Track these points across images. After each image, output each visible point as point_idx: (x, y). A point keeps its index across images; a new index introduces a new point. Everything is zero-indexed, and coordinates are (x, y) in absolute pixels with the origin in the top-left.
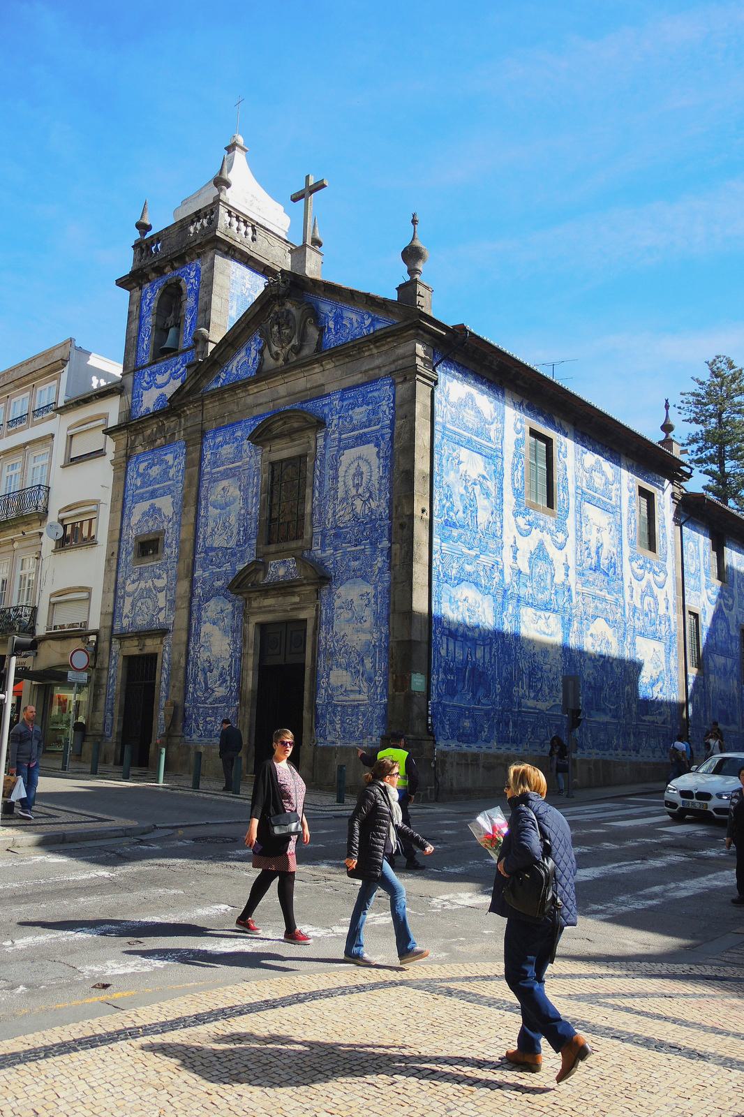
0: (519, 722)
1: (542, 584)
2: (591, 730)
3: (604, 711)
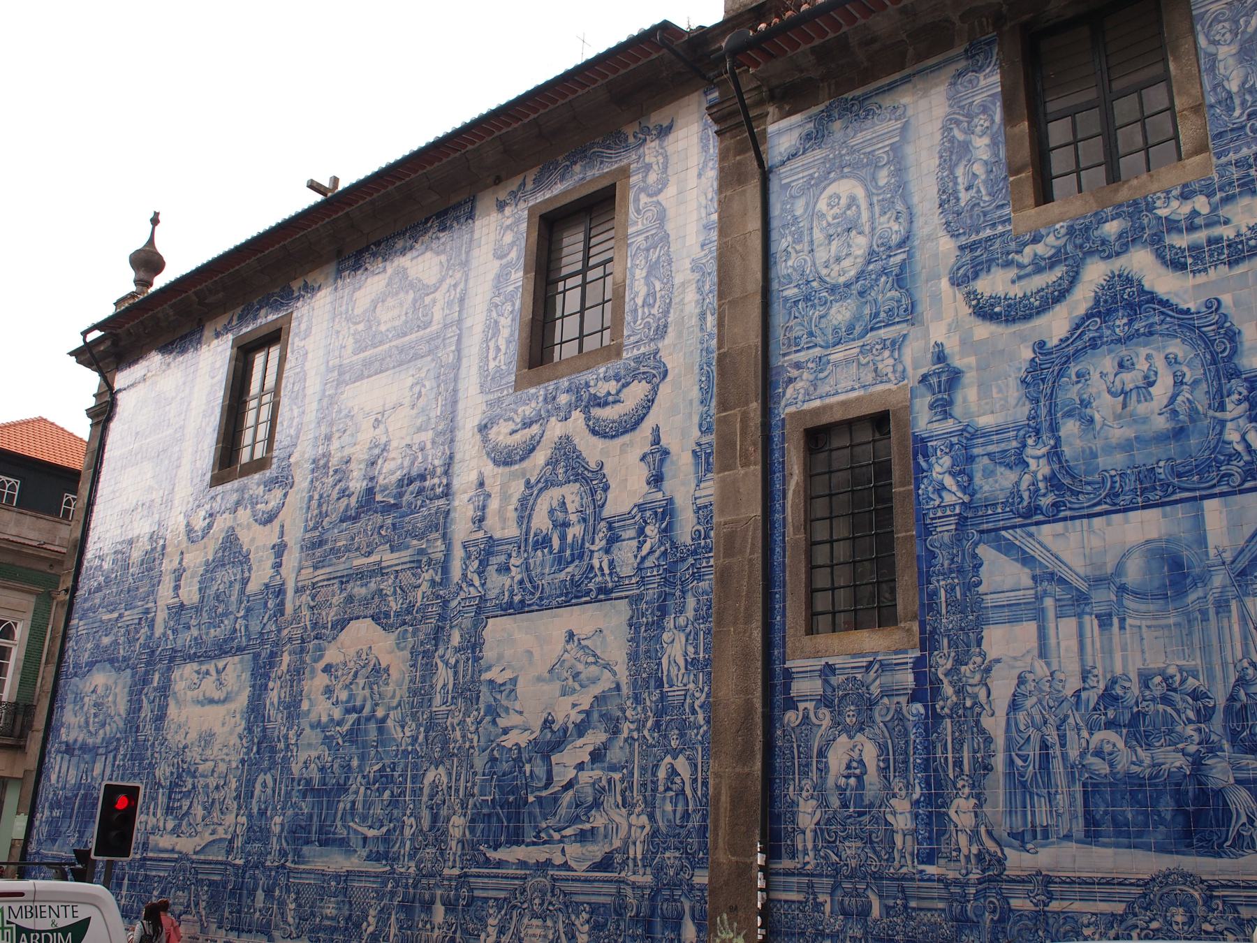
0: (140, 878)
1: (220, 610)
2: (298, 893)
3: (343, 843)
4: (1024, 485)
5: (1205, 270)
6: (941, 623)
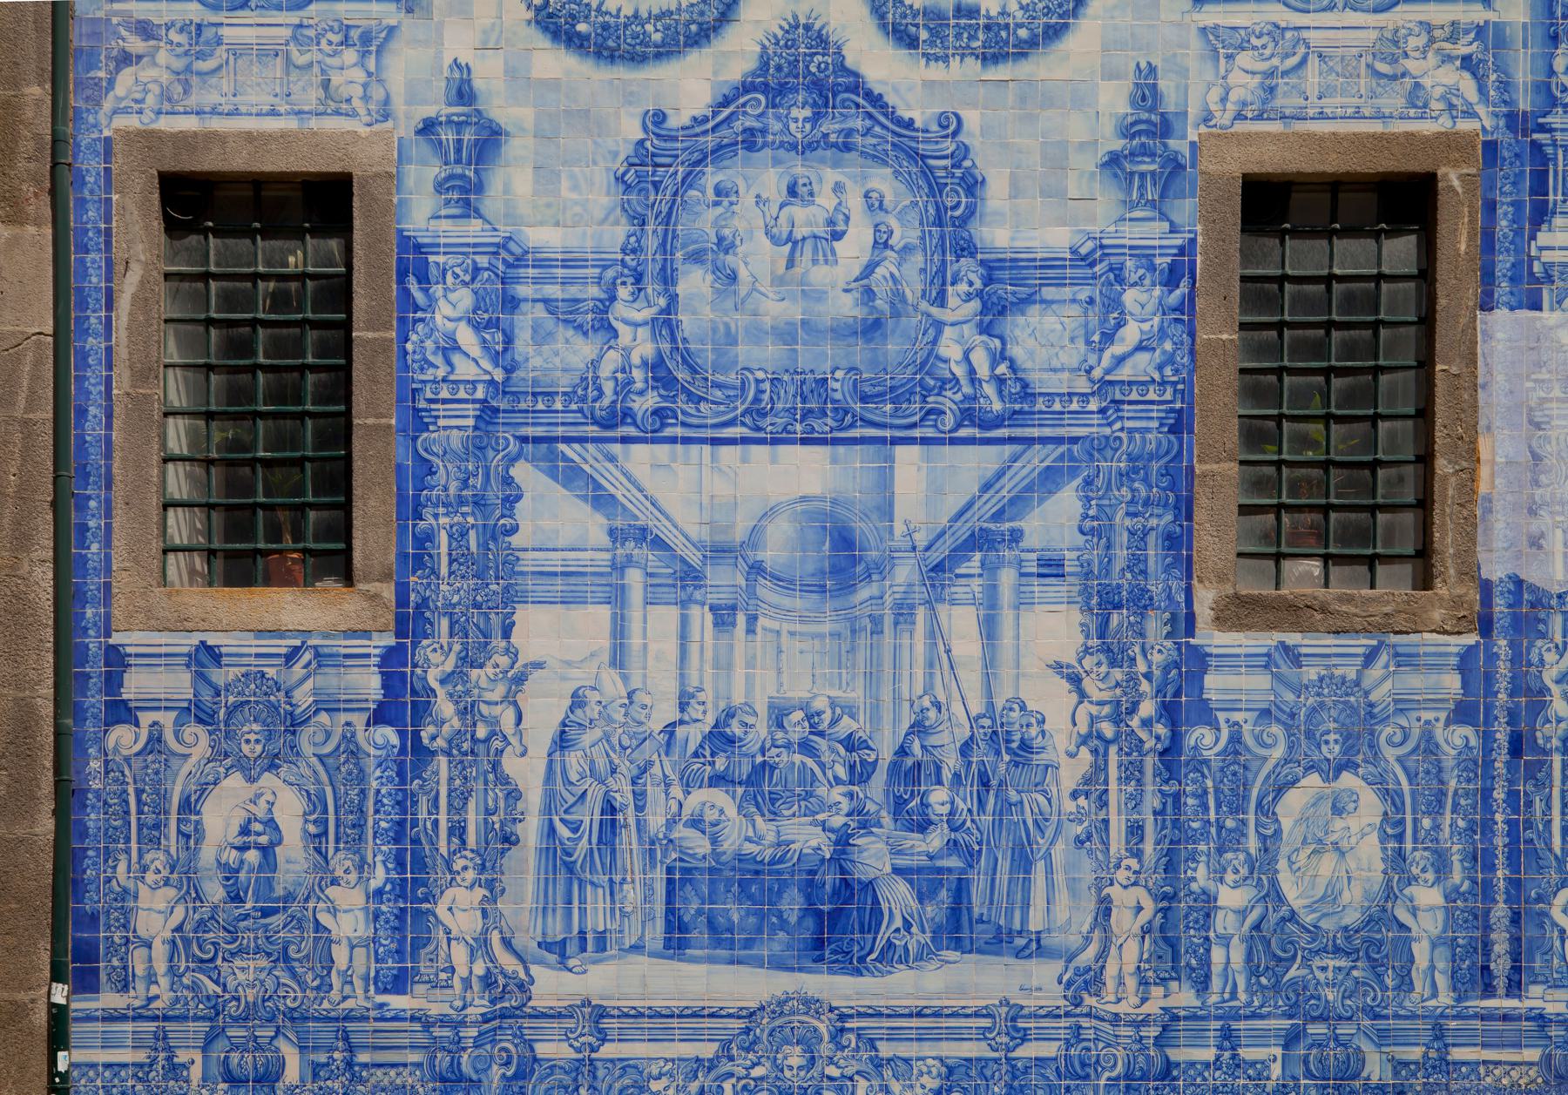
4: (606, 370)
5: (945, 59)
6: (437, 591)
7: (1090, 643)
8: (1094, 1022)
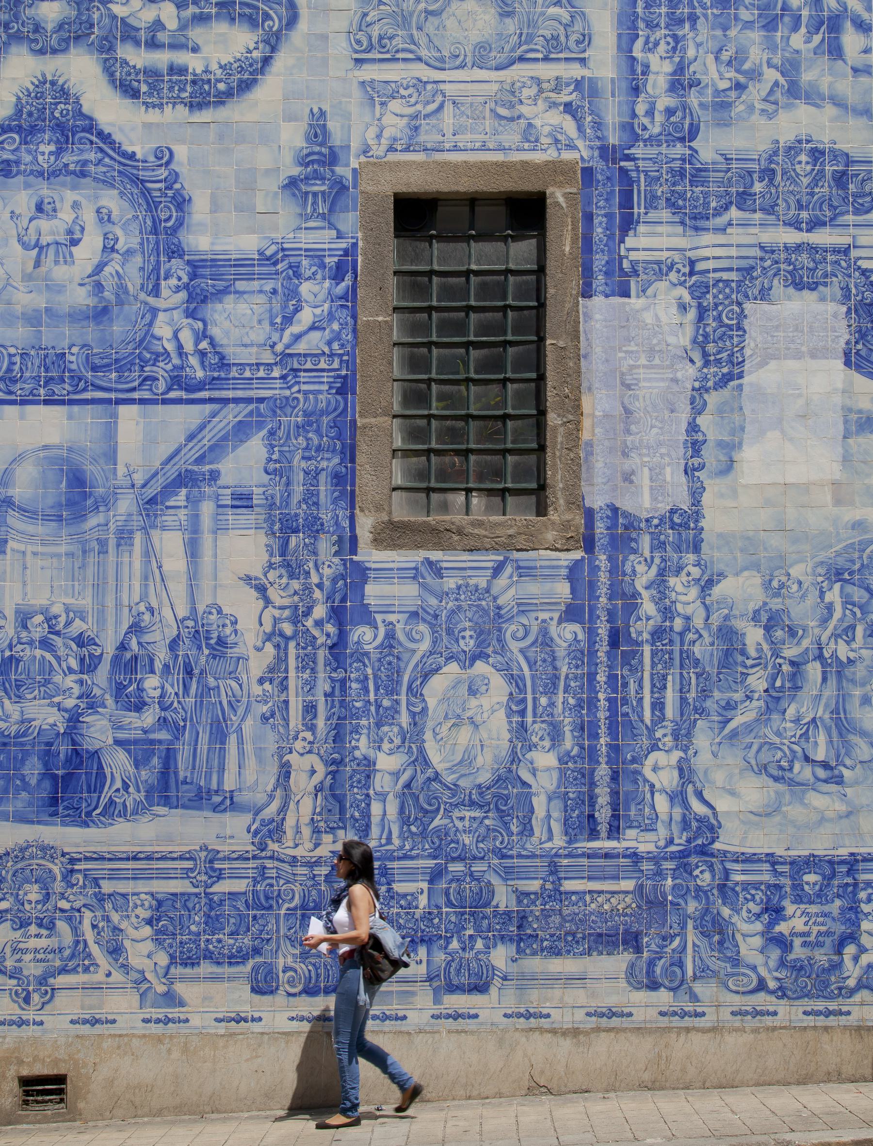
5: (161, 106)
7: (273, 560)
8: (276, 864)
